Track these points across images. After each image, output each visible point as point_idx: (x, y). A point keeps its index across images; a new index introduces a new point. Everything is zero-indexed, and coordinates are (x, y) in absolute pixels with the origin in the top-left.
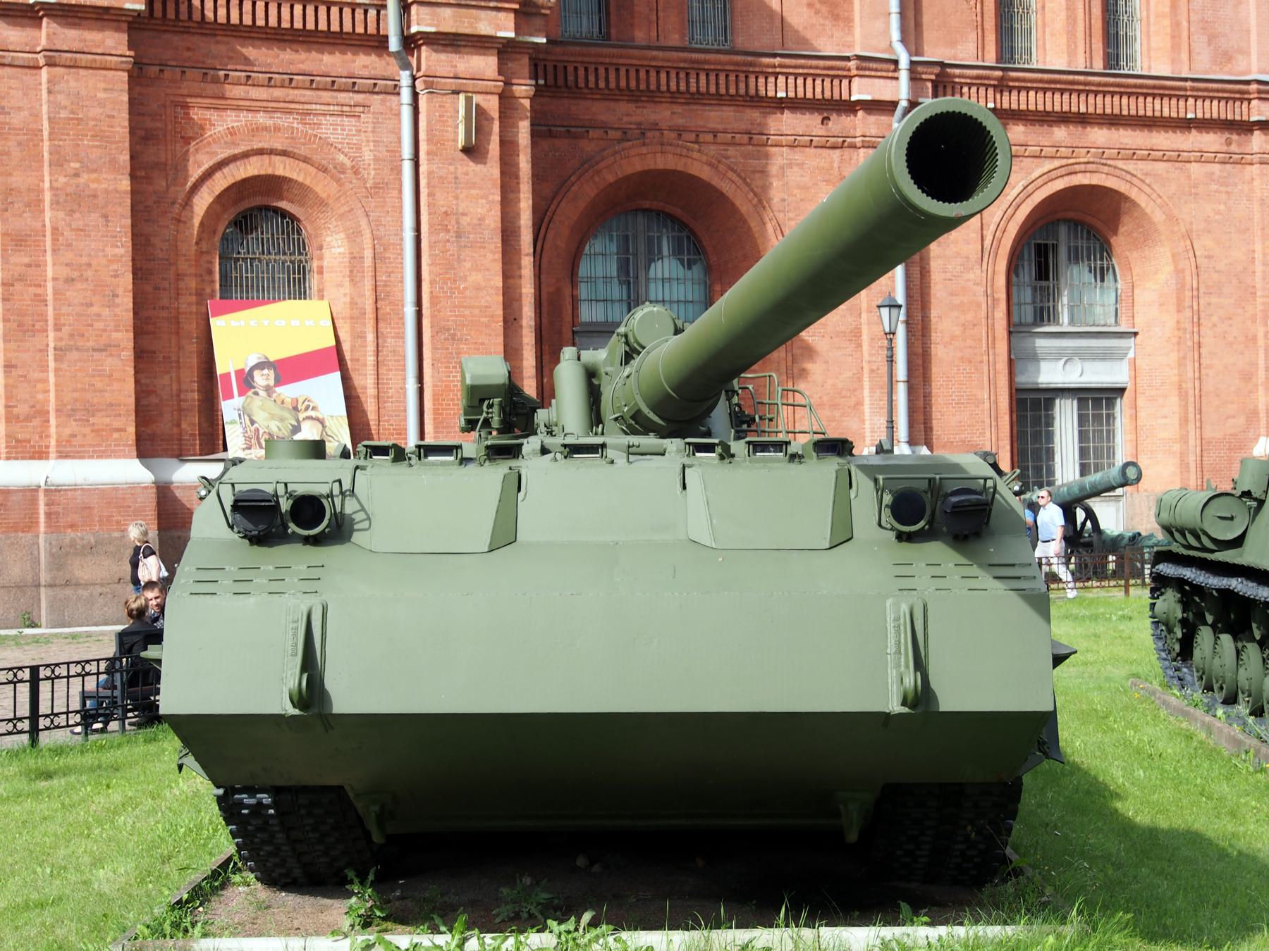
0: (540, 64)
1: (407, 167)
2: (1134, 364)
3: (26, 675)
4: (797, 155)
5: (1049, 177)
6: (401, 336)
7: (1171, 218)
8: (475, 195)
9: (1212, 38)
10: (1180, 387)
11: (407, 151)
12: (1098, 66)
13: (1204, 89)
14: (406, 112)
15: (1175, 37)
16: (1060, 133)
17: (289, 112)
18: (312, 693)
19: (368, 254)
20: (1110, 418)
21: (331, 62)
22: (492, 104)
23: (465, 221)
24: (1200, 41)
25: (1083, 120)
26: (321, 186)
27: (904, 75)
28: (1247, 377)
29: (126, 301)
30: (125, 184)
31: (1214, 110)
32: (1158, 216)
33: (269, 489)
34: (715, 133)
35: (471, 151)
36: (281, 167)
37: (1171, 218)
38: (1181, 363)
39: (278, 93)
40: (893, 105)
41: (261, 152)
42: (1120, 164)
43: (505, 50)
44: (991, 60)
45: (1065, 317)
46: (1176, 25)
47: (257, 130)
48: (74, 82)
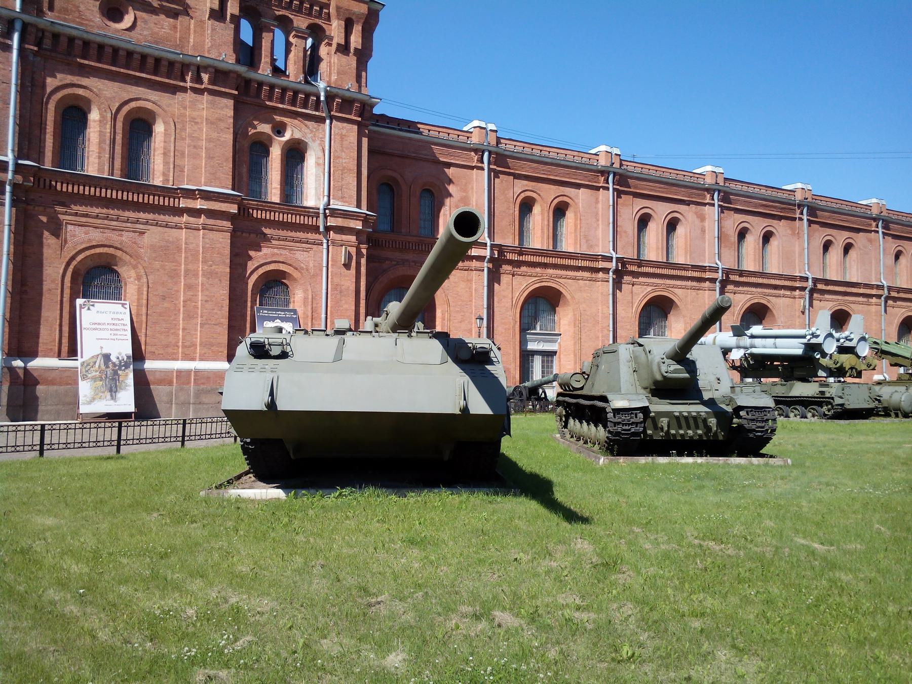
1: (324, 269)
3: (182, 422)
5: (534, 283)
8: (348, 280)
9: (587, 241)
11: (325, 264)
12: (551, 248)
13: (585, 257)
15: (576, 240)
16: (538, 270)
18: (272, 405)
19: (310, 297)
20: (552, 361)
22: (353, 251)
24: (583, 241)
25: (545, 266)
26: (295, 274)
27: (488, 248)
30: (228, 270)
32: (568, 297)
33: (262, 340)
35: (347, 266)
37: (573, 298)
38: (575, 344)
39: (282, 243)
40: (485, 257)
43: (357, 233)
44: (517, 244)
45: (538, 328)
46: (576, 236)
47: (273, 255)
48: (212, 235)
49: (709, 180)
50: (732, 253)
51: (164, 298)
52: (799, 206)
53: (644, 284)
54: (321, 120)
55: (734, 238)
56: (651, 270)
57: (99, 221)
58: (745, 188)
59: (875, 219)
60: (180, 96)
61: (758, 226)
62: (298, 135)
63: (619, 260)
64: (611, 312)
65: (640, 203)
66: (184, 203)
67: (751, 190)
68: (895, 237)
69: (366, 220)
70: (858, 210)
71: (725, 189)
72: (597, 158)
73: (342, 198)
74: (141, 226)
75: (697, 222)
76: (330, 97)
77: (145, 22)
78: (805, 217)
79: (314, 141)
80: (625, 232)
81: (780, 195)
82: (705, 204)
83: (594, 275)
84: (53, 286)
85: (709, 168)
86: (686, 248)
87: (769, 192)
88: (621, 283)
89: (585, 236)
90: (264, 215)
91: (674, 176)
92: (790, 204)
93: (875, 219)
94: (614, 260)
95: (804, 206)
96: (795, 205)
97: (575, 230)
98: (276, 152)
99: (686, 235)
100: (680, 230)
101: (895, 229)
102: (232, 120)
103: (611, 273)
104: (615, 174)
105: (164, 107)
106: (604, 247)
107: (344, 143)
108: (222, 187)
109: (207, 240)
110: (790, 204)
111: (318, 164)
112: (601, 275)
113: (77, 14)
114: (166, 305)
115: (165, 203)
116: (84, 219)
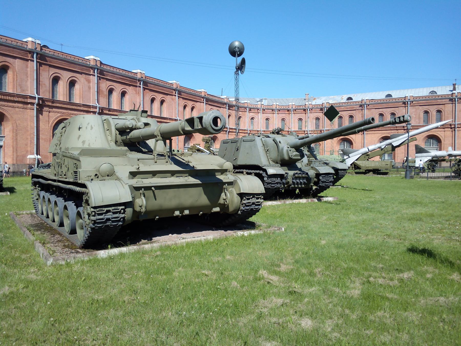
24: (18, 88)
28: (26, 145)
31: (21, 99)
32: (9, 116)
37: (12, 117)
38: (13, 142)
49: (92, 63)
50: (105, 100)
52: (139, 80)
53: (56, 112)
55: (106, 93)
56: (60, 105)
58: (112, 69)
59: (174, 90)
61: (118, 88)
63: (39, 99)
64: (35, 126)
65: (53, 71)
67: (115, 70)
68: (183, 98)
70: (167, 85)
71: (100, 68)
72: (26, 44)
75: (86, 83)
78: (142, 86)
80: (45, 84)
81: (130, 74)
82: (90, 75)
83: (25, 106)
85: (92, 57)
86: (80, 96)
87: (124, 73)
88: (42, 111)
89: (20, 85)
91: (73, 59)
92: (134, 79)
93: (174, 90)
94: (37, 99)
95: (141, 81)
96: (137, 80)
99: (80, 89)
100: (77, 86)
101: (184, 95)
103: (35, 106)
104: (37, 54)
106: (31, 91)
110: (134, 79)
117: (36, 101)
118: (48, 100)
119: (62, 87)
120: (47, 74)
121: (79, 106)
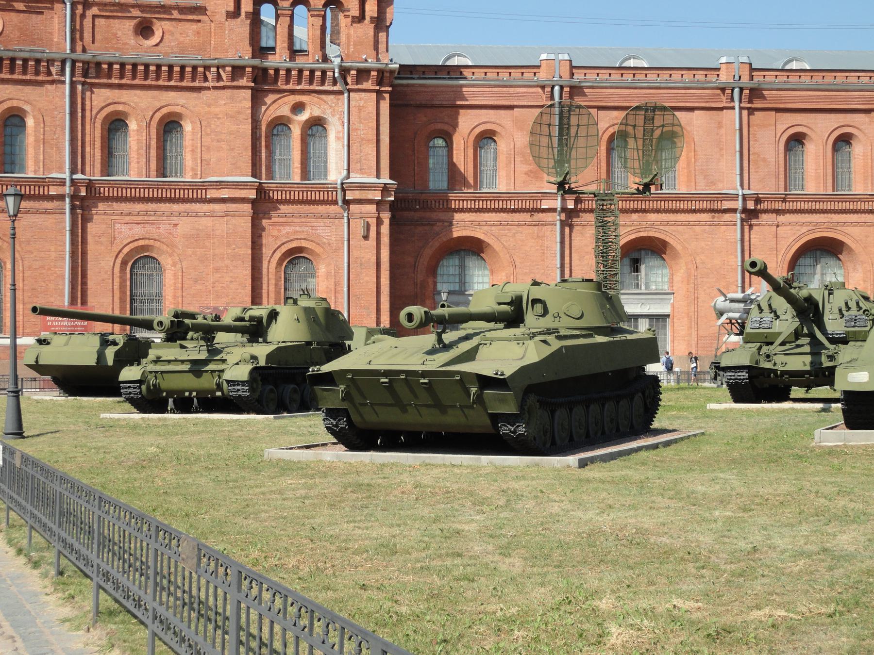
0: (393, 207)
1: (346, 243)
2: (673, 306)
4: (520, 229)
6: (343, 298)
7: (684, 248)
8: (366, 251)
10: (688, 315)
11: (346, 238)
14: (346, 225)
16: (635, 216)
17: (306, 226)
19: (333, 271)
20: (665, 327)
21: (321, 209)
22: (373, 222)
23: (363, 260)
26: (318, 250)
29: (250, 288)
30: (250, 251)
31: (705, 205)
32: (679, 247)
34: (486, 222)
35: (366, 237)
36: (304, 244)
37: (684, 248)
39: (303, 220)
41: (297, 239)
42: (661, 227)
43: (379, 203)
45: (643, 287)
47: (296, 232)
48: (234, 221)
51: (196, 281)
54: (341, 93)
57: (140, 218)
60: (205, 94)
62: (317, 113)
66: (212, 194)
69: (385, 189)
73: (361, 170)
74: (175, 218)
76: (344, 72)
77: (172, 34)
79: (333, 116)
80: (764, 160)
84: (106, 276)
90: (284, 196)
97: (688, 164)
98: (296, 131)
102: (250, 111)
105: (191, 108)
106: (729, 182)
107: (362, 114)
108: (243, 175)
109: (230, 226)
111: (338, 138)
112: (727, 217)
113: (114, 41)
114: (198, 287)
115: (194, 195)
116: (127, 218)
117: (739, 204)
118: (771, 198)
119: (815, 157)
120: (770, 133)
121: (860, 200)
